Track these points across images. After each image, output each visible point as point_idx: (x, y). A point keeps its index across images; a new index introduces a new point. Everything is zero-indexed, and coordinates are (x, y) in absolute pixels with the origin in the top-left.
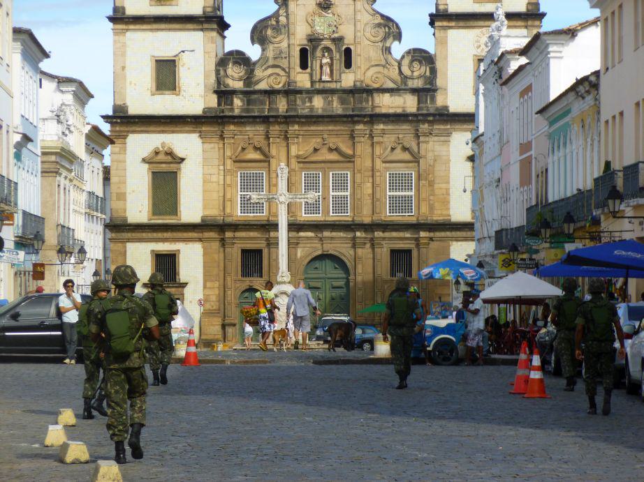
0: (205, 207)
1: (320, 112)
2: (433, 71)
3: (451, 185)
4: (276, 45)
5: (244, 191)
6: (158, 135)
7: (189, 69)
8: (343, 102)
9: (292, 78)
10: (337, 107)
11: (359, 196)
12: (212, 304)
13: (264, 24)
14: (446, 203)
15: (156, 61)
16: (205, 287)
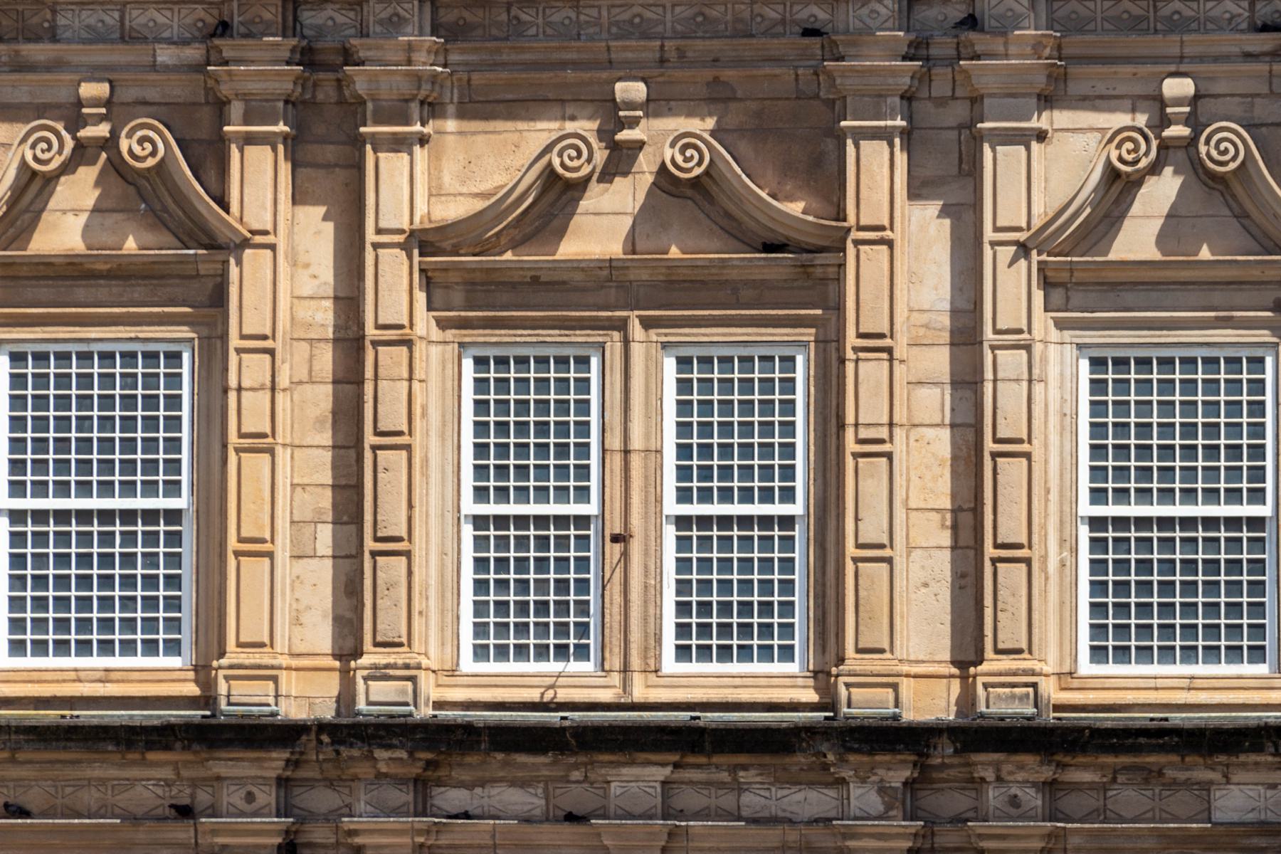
11: (873, 530)
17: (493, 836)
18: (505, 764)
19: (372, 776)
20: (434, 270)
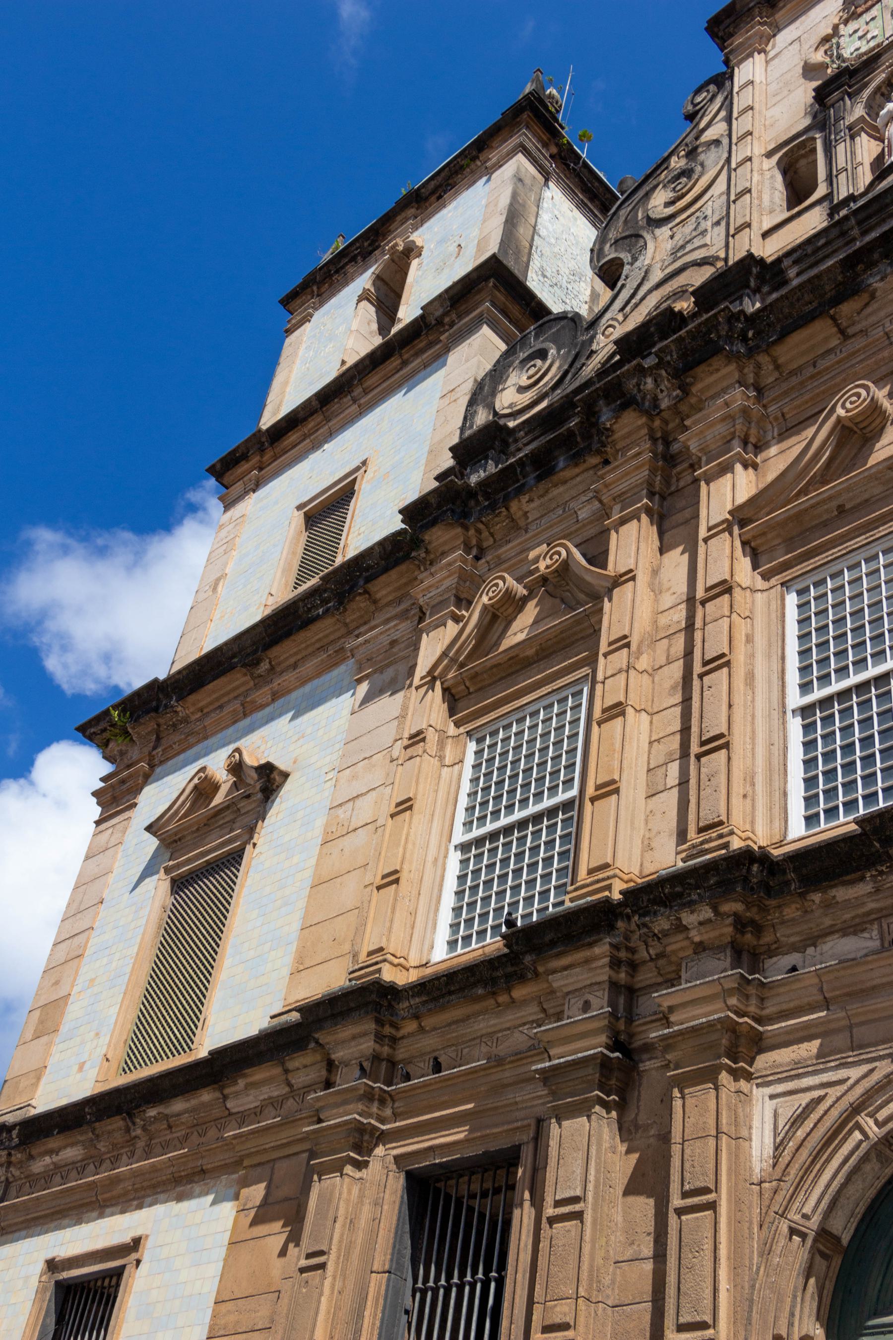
17: (821, 990)
18: (829, 905)
19: (690, 952)
20: (754, 537)
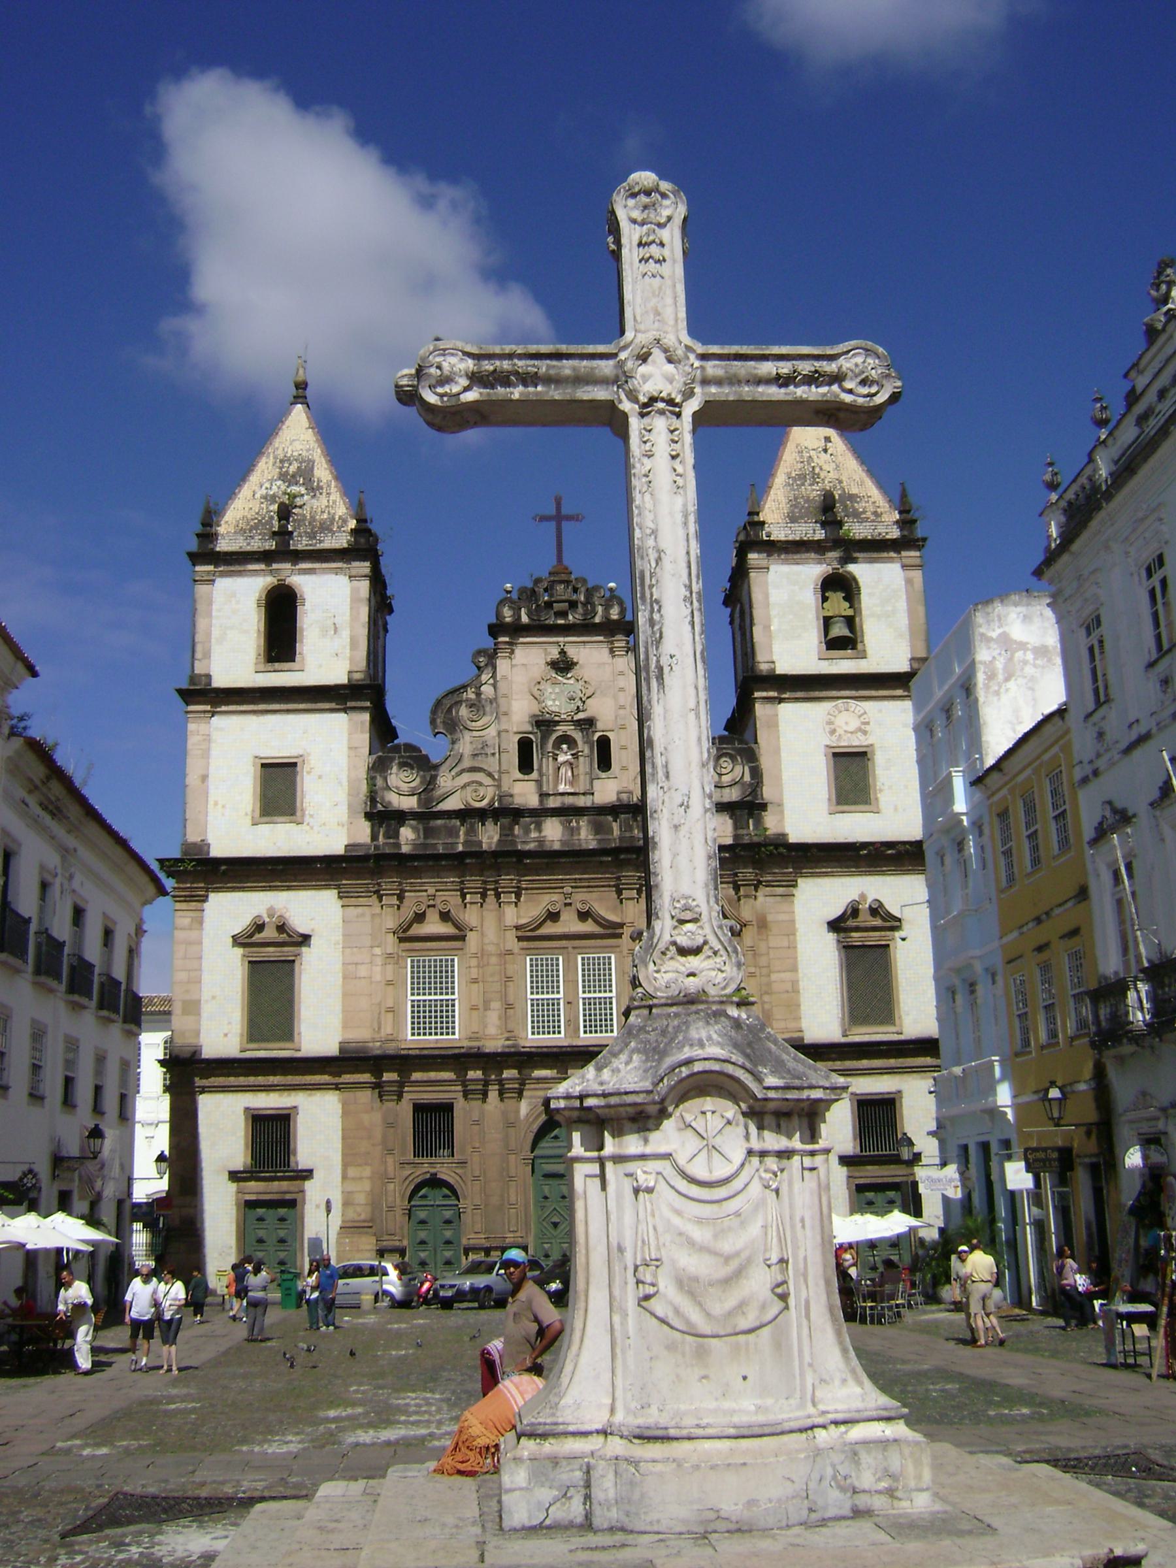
0: (346, 1026)
1: (557, 846)
2: (756, 773)
3: (801, 975)
4: (475, 734)
5: (419, 994)
6: (262, 894)
7: (320, 777)
8: (598, 829)
9: (505, 788)
10: (586, 837)
12: (359, 1209)
13: (456, 698)
14: (793, 1007)
15: (263, 765)
16: (344, 1177)
